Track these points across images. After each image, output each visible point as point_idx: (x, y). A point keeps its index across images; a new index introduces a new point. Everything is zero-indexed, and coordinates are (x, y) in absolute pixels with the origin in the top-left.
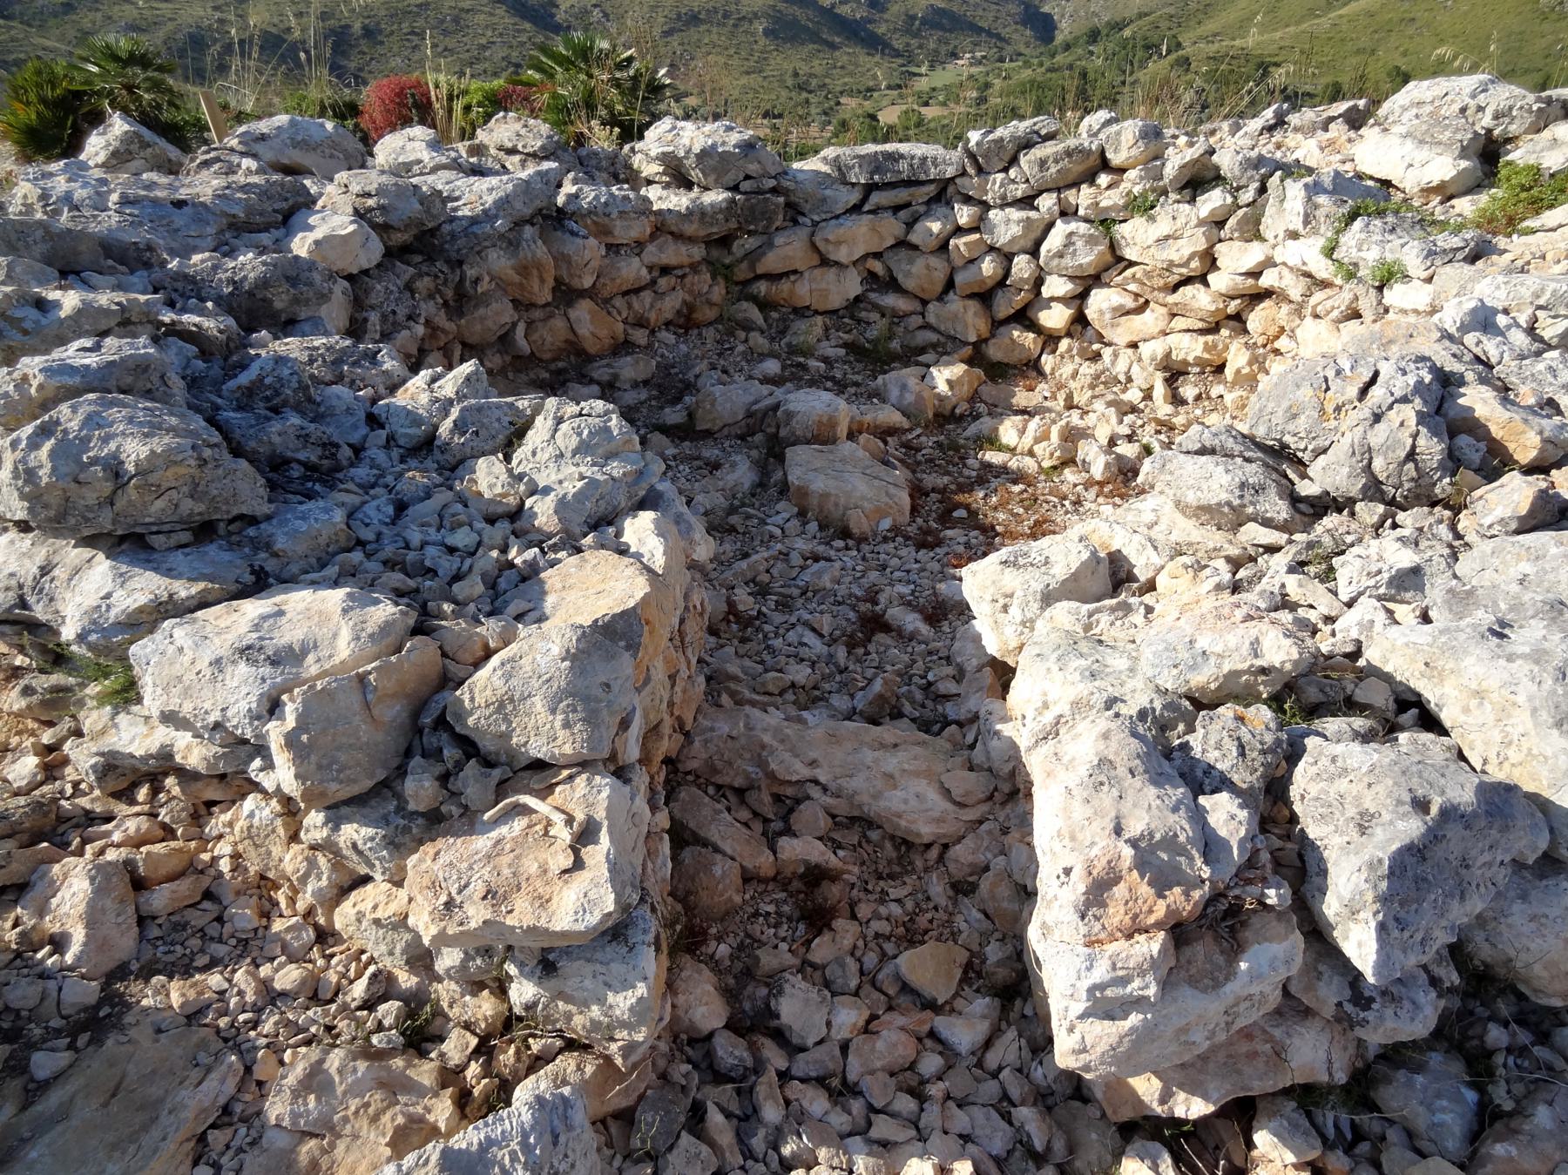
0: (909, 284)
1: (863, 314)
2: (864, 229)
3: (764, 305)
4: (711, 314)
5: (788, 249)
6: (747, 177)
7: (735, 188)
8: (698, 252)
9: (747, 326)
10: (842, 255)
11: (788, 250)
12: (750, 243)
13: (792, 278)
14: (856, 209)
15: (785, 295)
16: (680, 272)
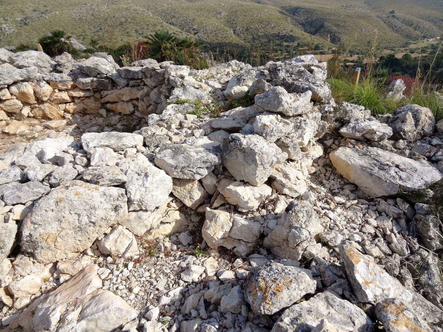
0: (140, 109)
1: (134, 117)
2: (128, 92)
3: (108, 111)
4: (93, 112)
5: (111, 95)
6: (98, 74)
7: (96, 77)
8: (88, 94)
9: (102, 116)
10: (125, 98)
11: (111, 96)
12: (106, 92)
13: (117, 104)
14: (127, 85)
15: (114, 108)
16: (81, 99)
